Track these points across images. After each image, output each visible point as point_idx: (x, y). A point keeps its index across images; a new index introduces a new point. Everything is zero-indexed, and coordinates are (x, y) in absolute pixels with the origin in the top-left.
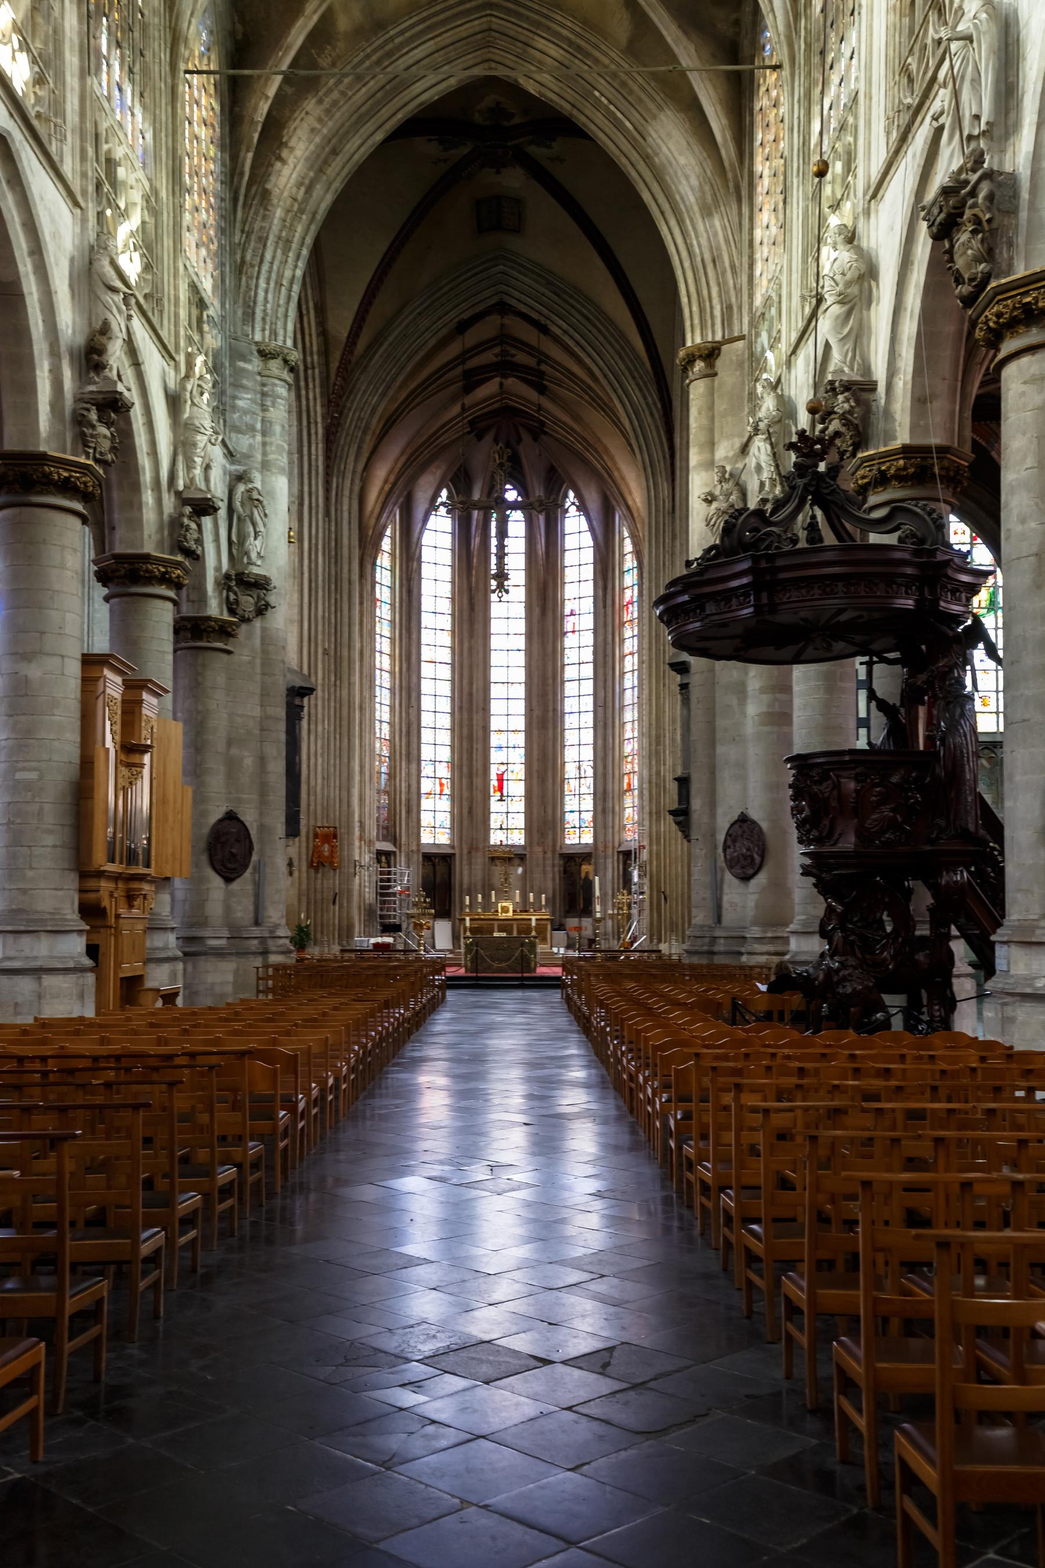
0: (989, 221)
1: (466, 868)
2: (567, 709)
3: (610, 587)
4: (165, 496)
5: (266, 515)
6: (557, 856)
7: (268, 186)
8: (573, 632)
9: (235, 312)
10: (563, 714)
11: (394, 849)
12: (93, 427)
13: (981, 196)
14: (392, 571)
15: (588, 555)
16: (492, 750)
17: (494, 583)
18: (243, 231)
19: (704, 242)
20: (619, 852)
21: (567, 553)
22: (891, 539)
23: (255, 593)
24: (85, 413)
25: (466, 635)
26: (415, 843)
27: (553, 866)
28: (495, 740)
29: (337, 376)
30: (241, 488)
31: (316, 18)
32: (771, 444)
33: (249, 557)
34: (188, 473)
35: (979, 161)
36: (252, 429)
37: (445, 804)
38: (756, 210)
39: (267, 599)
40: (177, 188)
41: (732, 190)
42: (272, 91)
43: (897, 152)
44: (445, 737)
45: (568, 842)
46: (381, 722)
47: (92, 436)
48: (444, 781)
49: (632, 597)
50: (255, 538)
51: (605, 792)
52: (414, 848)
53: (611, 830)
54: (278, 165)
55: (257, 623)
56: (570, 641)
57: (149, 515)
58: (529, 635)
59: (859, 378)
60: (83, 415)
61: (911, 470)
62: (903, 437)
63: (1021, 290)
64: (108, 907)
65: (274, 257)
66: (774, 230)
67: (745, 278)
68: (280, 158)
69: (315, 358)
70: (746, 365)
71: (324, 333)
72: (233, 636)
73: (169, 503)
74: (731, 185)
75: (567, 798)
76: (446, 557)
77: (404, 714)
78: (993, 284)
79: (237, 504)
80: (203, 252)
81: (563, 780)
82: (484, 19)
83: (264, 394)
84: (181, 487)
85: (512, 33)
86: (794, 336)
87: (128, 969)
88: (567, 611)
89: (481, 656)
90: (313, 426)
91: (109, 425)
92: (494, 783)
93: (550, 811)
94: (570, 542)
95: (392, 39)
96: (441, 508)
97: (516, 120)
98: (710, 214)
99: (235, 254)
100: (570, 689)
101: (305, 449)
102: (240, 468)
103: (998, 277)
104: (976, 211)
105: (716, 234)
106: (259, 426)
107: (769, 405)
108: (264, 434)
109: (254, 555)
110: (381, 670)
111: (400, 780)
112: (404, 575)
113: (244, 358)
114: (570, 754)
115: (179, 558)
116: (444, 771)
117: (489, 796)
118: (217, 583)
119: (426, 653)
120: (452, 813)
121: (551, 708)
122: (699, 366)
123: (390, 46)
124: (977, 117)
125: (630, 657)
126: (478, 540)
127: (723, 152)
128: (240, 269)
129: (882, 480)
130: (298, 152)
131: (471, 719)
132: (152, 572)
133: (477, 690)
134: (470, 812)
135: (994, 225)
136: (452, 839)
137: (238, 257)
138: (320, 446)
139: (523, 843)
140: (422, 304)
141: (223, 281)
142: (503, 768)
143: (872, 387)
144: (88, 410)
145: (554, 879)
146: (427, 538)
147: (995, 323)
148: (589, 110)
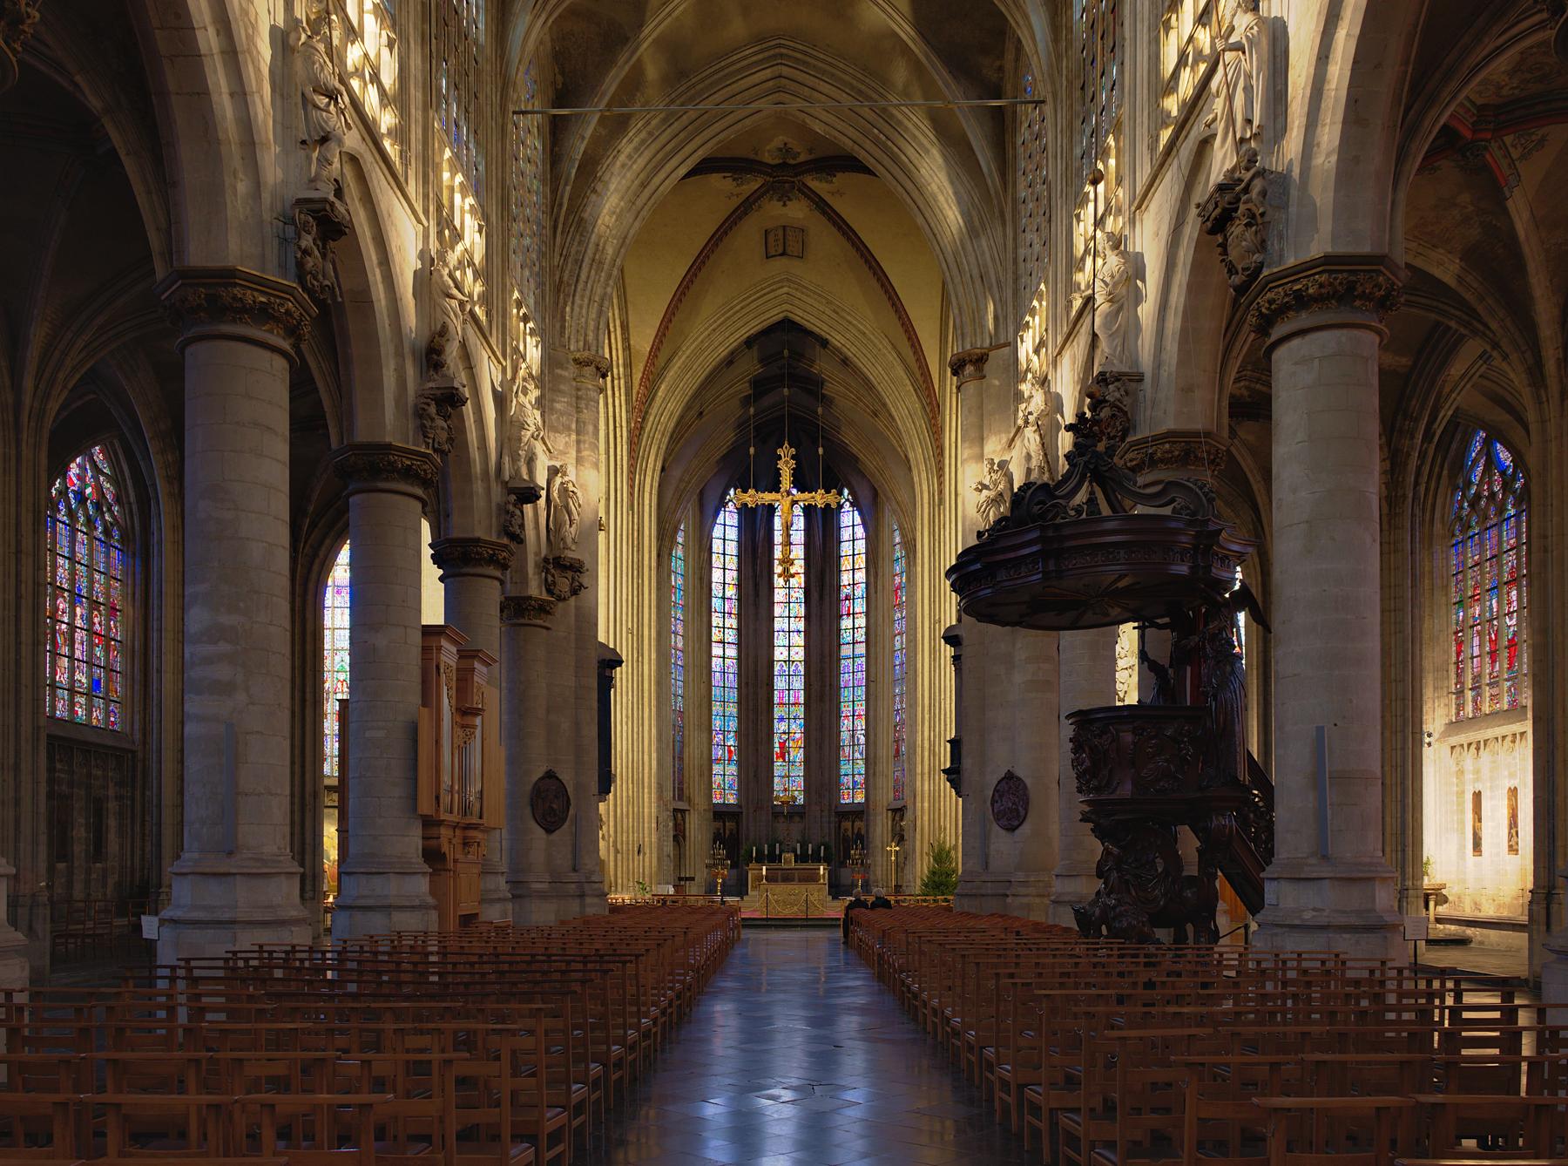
0: (1262, 215)
2: (842, 685)
4: (493, 484)
5: (580, 506)
7: (586, 215)
8: (848, 615)
9: (554, 326)
12: (433, 420)
13: (1254, 193)
15: (861, 546)
17: (778, 569)
18: (561, 255)
19: (972, 260)
22: (1167, 511)
23: (570, 574)
24: (426, 407)
28: (778, 712)
29: (640, 385)
30: (558, 480)
31: (627, 68)
32: (1041, 435)
33: (565, 543)
34: (513, 465)
35: (1252, 161)
36: (569, 429)
38: (1020, 231)
39: (580, 580)
40: (506, 214)
41: (997, 214)
42: (588, 133)
43: (1162, 165)
44: (732, 709)
46: (676, 696)
47: (431, 427)
48: (732, 748)
50: (571, 526)
54: (593, 197)
55: (573, 599)
56: (846, 623)
57: (479, 503)
59: (1127, 370)
60: (424, 409)
61: (1177, 453)
62: (1169, 424)
63: (1292, 278)
64: (447, 852)
65: (588, 277)
66: (1037, 247)
67: (1009, 292)
68: (594, 191)
69: (621, 369)
70: (1012, 368)
71: (627, 347)
72: (548, 613)
73: (497, 492)
74: (996, 210)
78: (1265, 272)
79: (555, 494)
80: (527, 273)
82: (775, 68)
83: (578, 398)
84: (507, 478)
85: (800, 79)
86: (1060, 340)
87: (467, 908)
88: (843, 596)
90: (618, 430)
91: (446, 417)
92: (777, 750)
94: (846, 534)
95: (694, 85)
96: (730, 504)
97: (802, 158)
98: (977, 236)
99: (554, 275)
101: (612, 451)
102: (558, 464)
103: (1269, 266)
104: (1249, 206)
105: (983, 253)
106: (574, 426)
107: (1037, 402)
108: (578, 433)
109: (569, 541)
113: (561, 366)
114: (846, 724)
115: (505, 541)
118: (537, 565)
119: (716, 635)
122: (969, 369)
123: (693, 91)
124: (1249, 121)
127: (989, 182)
128: (558, 288)
129: (1152, 462)
130: (612, 187)
132: (481, 554)
135: (1267, 219)
137: (557, 278)
138: (625, 447)
140: (715, 322)
141: (543, 298)
143: (1139, 378)
144: (428, 405)
146: (717, 532)
147: (1268, 309)
148: (868, 145)
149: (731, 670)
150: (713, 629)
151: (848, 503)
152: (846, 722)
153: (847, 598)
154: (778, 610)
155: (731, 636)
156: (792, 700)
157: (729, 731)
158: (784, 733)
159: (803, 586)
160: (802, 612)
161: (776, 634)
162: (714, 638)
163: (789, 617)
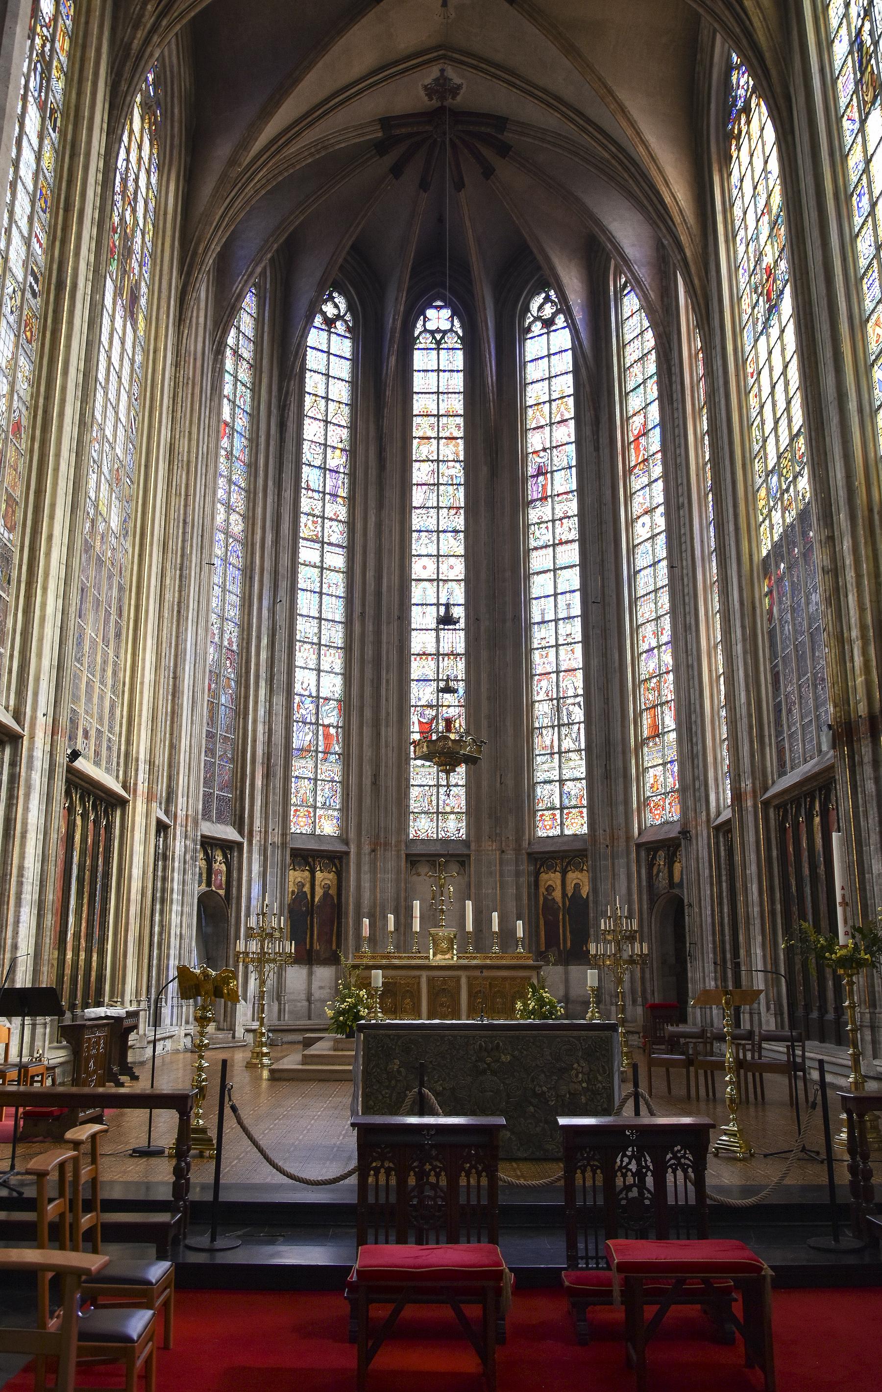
1: (366, 878)
2: (536, 617)
3: (604, 418)
6: (525, 857)
8: (544, 499)
10: (529, 625)
11: (238, 838)
14: (255, 389)
20: (639, 846)
21: (529, 388)
25: (372, 504)
26: (278, 831)
27: (518, 874)
37: (332, 770)
44: (334, 661)
45: (541, 833)
48: (332, 731)
49: (645, 425)
51: (608, 742)
52: (277, 839)
53: (621, 808)
58: (471, 509)
76: (341, 391)
77: (265, 613)
81: (531, 730)
88: (531, 470)
89: (396, 537)
93: (510, 782)
100: (540, 585)
110: (227, 533)
111: (255, 721)
112: (274, 401)
114: (542, 689)
116: (331, 716)
120: (345, 783)
121: (509, 616)
125: (646, 519)
126: (393, 360)
131: (378, 633)
133: (389, 588)
134: (375, 783)
136: (344, 826)
145: (518, 898)
149: (332, 590)
150: (303, 519)
151: (539, 324)
152: (544, 683)
153: (540, 472)
154: (418, 496)
155: (336, 533)
156: (445, 648)
158: (430, 706)
159: (462, 458)
161: (415, 535)
162: (304, 532)
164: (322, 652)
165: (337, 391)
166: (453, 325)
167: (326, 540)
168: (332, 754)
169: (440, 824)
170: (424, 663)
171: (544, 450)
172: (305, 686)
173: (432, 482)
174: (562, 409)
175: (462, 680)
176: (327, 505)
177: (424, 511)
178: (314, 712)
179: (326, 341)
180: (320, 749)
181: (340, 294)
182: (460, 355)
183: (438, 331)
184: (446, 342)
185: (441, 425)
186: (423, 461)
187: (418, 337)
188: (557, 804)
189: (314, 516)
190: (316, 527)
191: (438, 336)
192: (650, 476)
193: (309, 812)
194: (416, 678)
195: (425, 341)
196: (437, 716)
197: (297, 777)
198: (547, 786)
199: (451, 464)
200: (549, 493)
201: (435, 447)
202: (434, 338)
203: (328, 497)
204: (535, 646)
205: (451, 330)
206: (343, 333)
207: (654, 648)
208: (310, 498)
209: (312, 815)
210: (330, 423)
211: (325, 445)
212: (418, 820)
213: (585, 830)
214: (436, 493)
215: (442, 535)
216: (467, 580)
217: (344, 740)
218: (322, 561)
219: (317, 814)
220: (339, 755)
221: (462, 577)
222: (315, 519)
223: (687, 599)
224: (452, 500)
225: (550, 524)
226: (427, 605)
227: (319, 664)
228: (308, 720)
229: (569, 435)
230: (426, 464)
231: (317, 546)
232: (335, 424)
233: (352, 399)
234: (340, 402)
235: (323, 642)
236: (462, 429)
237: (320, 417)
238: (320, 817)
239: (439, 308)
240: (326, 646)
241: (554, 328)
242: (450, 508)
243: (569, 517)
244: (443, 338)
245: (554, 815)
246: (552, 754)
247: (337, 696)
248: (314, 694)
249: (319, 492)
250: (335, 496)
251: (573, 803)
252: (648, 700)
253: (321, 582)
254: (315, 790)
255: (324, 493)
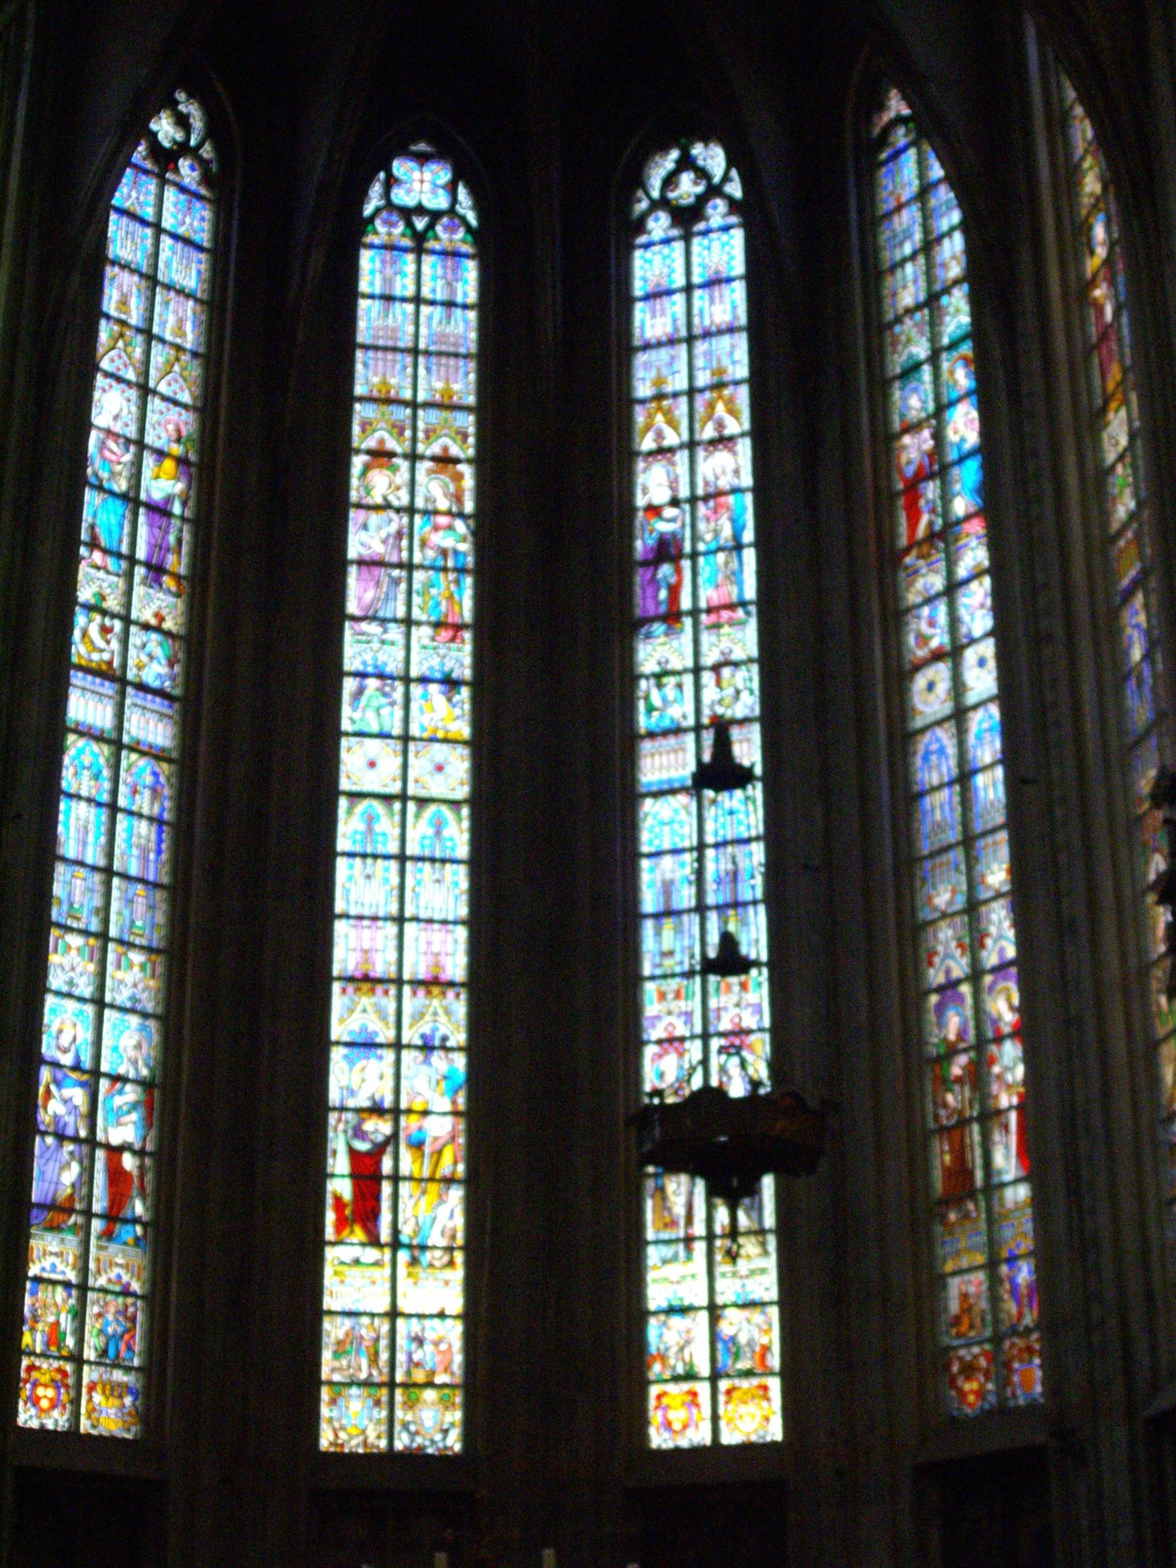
2: (649, 901)
8: (672, 617)
16: (337, 1055)
48: (128, 1162)
75: (653, 1254)
88: (641, 546)
117: (319, 1244)
120: (156, 1299)
125: (940, 672)
139: (454, 1441)
142: (380, 1128)
149: (144, 803)
150: (80, 619)
156: (416, 966)
157: (118, 1079)
158: (377, 1110)
159: (469, 506)
160: (467, 609)
161: (349, 685)
163: (408, 622)
164: (111, 957)
165: (171, 319)
166: (454, 201)
167: (131, 675)
168: (126, 1221)
169: (399, 1414)
170: (365, 1001)
171: (675, 502)
172: (65, 1041)
173: (394, 559)
174: (720, 409)
175: (460, 1049)
176: (139, 591)
177: (373, 628)
178: (84, 1108)
179: (151, 199)
180: (98, 1206)
181: (191, 95)
182: (470, 271)
183: (420, 210)
184: (436, 238)
185: (421, 425)
186: (377, 508)
187: (371, 219)
188: (704, 1370)
189: (104, 613)
190: (108, 642)
191: (420, 224)
192: (950, 573)
193: (64, 1374)
194: (346, 1038)
195: (381, 232)
196: (394, 1138)
197: (38, 1280)
198: (676, 1321)
199: (443, 520)
200: (686, 603)
201: (403, 476)
202: (410, 225)
203: (140, 572)
204: (647, 969)
205: (452, 211)
206: (194, 187)
207: (958, 982)
208: (98, 568)
209: (70, 1381)
210: (155, 392)
211: (141, 445)
212: (341, 1402)
213: (775, 1432)
214: (403, 586)
215: (416, 690)
216: (477, 801)
217: (158, 1191)
218: (119, 727)
219: (85, 1381)
220: (145, 1225)
221: (463, 792)
222: (107, 621)
223: (1062, 859)
224: (444, 606)
225: (688, 680)
226: (375, 857)
227: (101, 987)
228: (70, 1131)
229: (737, 472)
230: (383, 515)
231: (108, 688)
232: (165, 399)
233: (209, 345)
234: (179, 348)
235: (113, 932)
236: (471, 440)
237: (131, 375)
238: (92, 1388)
239: (422, 159)
240: (121, 942)
241: (701, 226)
242: (437, 625)
243: (736, 665)
244: (431, 226)
245: (694, 1394)
246: (689, 1240)
247: (145, 1072)
248: (87, 1063)
249: (119, 556)
250: (156, 570)
251: (743, 1364)
252: (945, 1105)
253: (115, 780)
254: (79, 1315)
255: (132, 560)
